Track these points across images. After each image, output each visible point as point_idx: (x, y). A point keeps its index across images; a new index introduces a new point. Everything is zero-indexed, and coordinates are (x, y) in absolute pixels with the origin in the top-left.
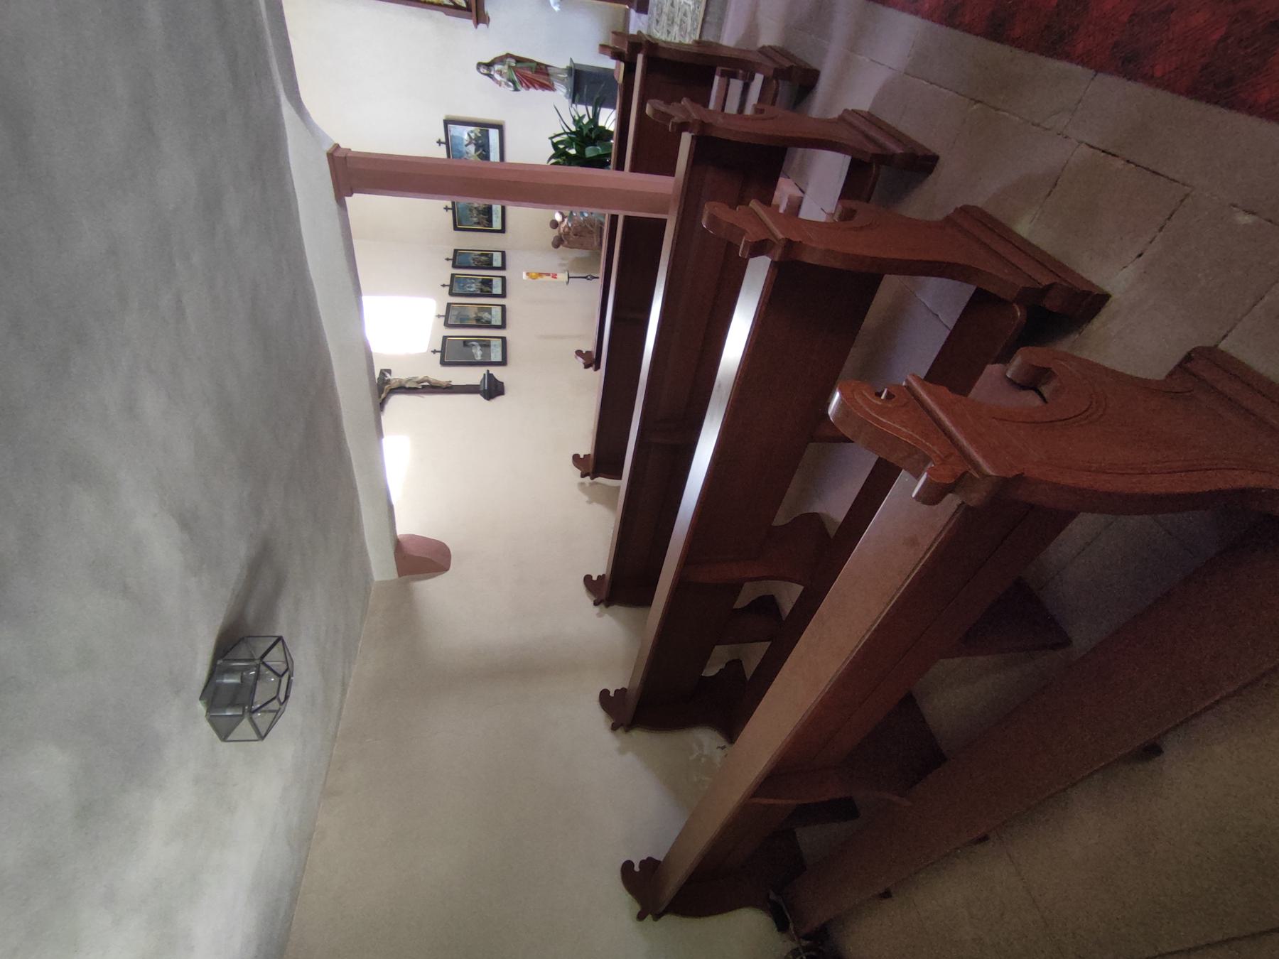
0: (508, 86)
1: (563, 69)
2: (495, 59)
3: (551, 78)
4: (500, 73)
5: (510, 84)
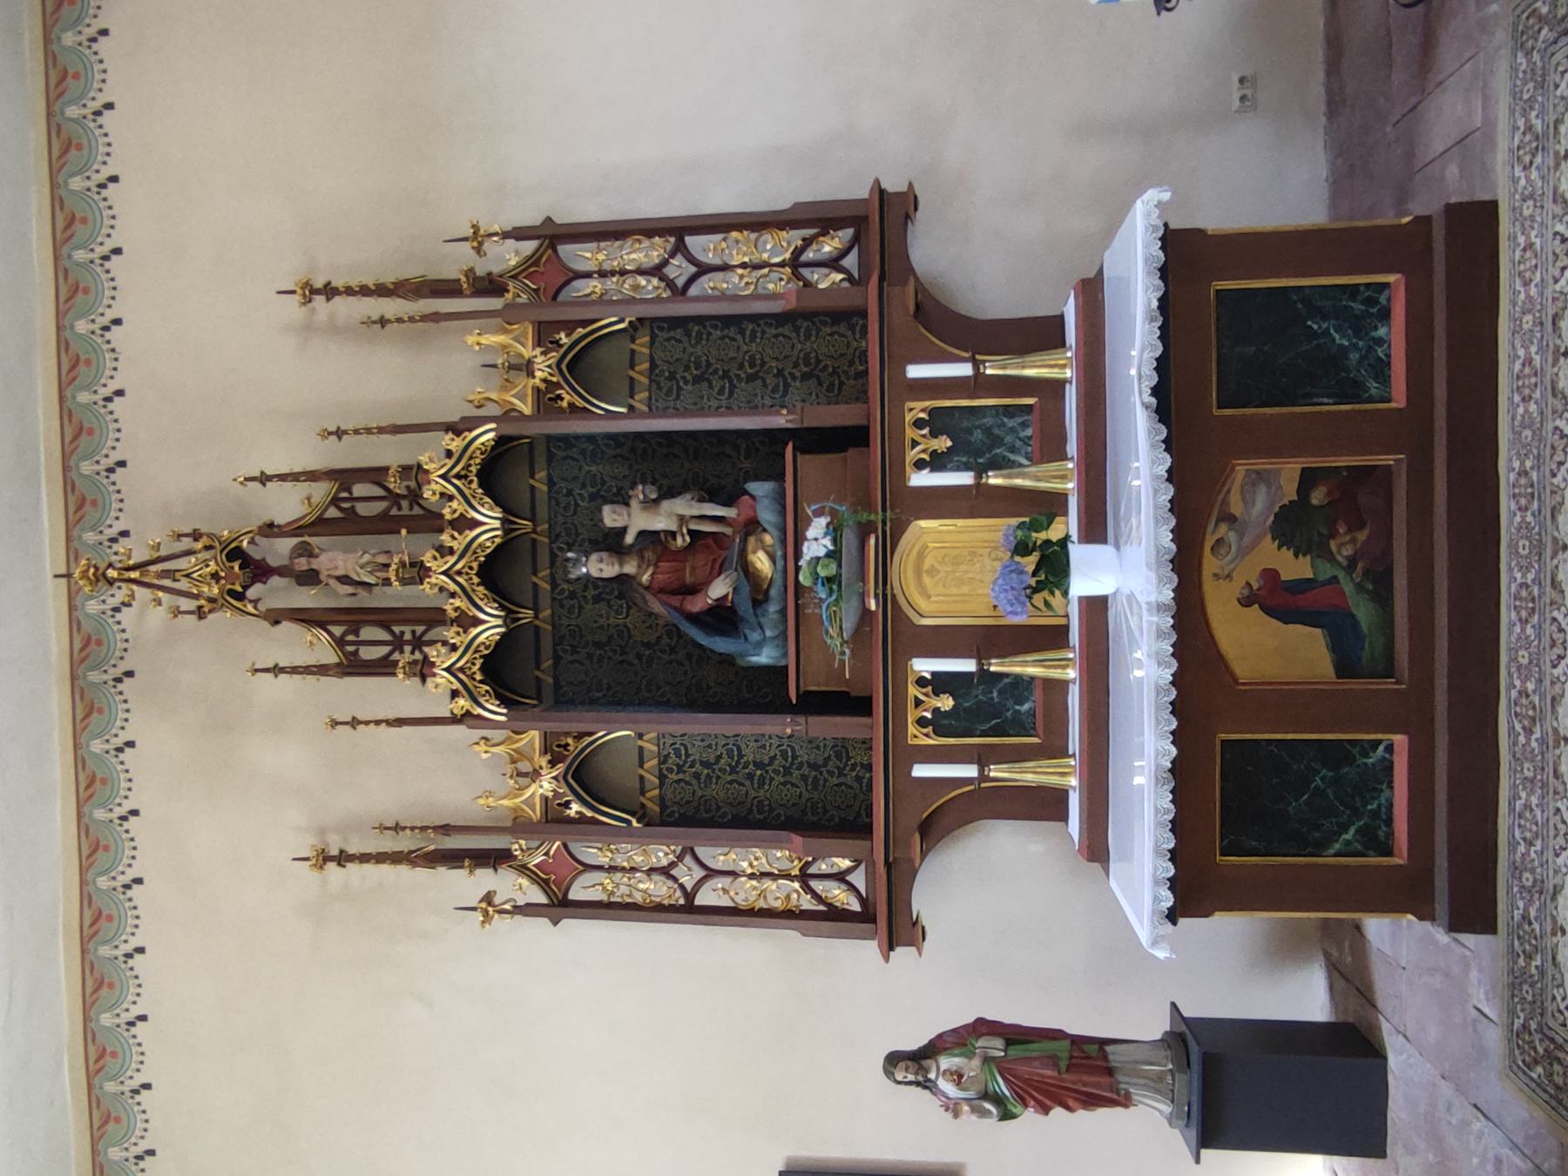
0: (984, 1113)
4: (957, 1077)
5: (988, 1106)
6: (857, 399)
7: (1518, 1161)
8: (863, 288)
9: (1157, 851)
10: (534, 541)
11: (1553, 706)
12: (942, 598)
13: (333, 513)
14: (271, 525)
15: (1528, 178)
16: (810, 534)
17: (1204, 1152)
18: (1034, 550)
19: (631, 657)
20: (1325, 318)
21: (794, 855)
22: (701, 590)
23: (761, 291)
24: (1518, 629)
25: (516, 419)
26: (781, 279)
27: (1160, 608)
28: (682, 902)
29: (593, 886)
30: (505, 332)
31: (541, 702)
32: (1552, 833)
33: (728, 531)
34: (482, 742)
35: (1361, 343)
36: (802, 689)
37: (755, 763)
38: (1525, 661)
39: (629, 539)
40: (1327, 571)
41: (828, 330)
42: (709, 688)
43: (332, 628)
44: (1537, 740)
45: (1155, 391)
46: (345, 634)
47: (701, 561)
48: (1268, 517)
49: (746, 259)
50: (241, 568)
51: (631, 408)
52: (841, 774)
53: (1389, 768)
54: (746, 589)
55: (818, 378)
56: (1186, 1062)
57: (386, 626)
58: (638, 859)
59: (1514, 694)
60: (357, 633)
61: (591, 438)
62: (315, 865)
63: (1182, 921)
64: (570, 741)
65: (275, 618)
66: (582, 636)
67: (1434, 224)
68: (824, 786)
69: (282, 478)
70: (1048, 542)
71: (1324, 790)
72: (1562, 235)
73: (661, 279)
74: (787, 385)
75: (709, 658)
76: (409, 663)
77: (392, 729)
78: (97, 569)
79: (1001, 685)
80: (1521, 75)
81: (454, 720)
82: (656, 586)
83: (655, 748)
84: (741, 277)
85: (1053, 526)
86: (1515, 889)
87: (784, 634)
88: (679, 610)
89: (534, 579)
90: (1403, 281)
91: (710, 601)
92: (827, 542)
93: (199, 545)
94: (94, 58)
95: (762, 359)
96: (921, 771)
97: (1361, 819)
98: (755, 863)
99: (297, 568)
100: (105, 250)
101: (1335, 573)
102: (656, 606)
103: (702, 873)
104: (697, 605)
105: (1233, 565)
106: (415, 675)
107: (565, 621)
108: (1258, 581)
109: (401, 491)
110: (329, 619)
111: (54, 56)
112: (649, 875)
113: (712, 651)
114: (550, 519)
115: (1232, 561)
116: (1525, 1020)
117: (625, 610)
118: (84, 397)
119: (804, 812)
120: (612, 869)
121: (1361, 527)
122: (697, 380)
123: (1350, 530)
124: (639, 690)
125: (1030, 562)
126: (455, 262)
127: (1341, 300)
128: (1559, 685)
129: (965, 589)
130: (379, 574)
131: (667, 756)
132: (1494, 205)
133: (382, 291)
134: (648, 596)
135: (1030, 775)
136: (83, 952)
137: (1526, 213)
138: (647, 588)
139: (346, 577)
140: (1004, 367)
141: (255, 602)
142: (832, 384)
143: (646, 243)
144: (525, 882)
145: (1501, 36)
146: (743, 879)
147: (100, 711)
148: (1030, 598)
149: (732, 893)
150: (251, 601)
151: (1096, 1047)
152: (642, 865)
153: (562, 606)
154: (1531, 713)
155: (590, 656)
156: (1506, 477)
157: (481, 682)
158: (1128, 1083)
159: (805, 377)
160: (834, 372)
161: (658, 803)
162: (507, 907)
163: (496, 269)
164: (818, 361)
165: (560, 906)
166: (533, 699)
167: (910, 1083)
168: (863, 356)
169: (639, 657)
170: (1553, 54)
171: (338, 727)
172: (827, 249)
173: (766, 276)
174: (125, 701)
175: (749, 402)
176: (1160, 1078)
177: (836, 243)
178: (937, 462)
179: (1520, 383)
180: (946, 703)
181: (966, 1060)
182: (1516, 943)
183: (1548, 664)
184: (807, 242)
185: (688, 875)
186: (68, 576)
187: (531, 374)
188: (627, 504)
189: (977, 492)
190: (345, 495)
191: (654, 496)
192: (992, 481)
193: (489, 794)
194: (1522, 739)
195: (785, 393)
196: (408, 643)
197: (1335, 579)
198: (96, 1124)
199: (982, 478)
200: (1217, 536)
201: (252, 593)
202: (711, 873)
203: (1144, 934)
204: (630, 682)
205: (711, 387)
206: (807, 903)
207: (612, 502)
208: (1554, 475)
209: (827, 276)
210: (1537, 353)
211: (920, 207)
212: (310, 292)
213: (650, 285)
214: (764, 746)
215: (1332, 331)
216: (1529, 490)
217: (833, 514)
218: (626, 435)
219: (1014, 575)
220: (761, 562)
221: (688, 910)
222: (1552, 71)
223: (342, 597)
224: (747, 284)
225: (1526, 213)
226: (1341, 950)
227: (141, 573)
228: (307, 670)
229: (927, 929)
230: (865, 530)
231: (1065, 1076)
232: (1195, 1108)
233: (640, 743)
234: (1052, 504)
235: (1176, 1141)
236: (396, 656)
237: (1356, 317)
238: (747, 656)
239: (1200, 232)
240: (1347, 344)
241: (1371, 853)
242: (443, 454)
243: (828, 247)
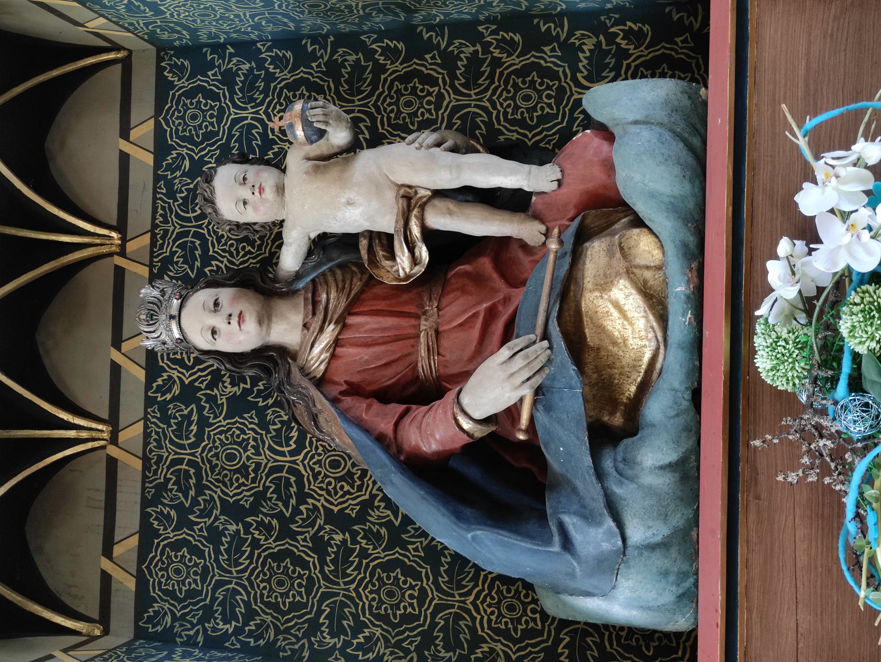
82: (341, 378)
114: (154, 226)
153: (165, 419)
188: (279, 164)
204: (296, 606)
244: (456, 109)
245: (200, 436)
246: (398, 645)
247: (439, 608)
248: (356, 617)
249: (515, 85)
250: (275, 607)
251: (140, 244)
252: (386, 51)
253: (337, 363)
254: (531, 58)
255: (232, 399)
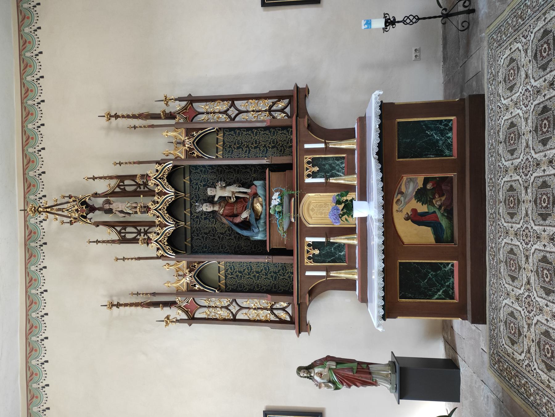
0: (329, 387)
1: (386, 365)
2: (315, 361)
3: (374, 376)
4: (320, 375)
5: (330, 384)
6: (290, 154)
7: (492, 396)
8: (291, 119)
9: (379, 297)
10: (185, 200)
11: (499, 251)
12: (316, 218)
13: (118, 190)
14: (96, 194)
15: (492, 89)
16: (273, 198)
17: (400, 400)
18: (342, 203)
19: (216, 237)
20: (432, 130)
21: (268, 302)
22: (239, 216)
23: (259, 120)
24: (490, 228)
25: (178, 160)
26: (265, 116)
27: (379, 220)
28: (232, 318)
29: (203, 313)
30: (176, 131)
31: (186, 252)
32: (499, 290)
33: (248, 196)
34: (167, 265)
35: (443, 138)
36: (271, 248)
37: (256, 272)
38: (492, 238)
39: (216, 199)
40: (432, 209)
41: (281, 132)
42: (242, 247)
43: (116, 228)
44: (495, 262)
45: (377, 154)
46: (121, 230)
47: (239, 206)
48: (413, 192)
49: (254, 109)
50: (86, 208)
51: (217, 157)
52: (284, 275)
53: (452, 272)
54: (253, 216)
55: (277, 148)
56: (395, 371)
57: (135, 227)
58: (218, 303)
59: (490, 248)
60: (125, 230)
61: (204, 166)
62: (109, 307)
63: (387, 320)
64: (196, 264)
65: (97, 224)
66: (200, 231)
67: (466, 101)
68: (278, 279)
69: (101, 178)
70: (347, 200)
71: (432, 278)
72: (499, 106)
73: (226, 115)
74: (267, 150)
75: (242, 238)
76: (143, 239)
77: (137, 261)
78: (35, 208)
79: (335, 246)
80: (490, 56)
81: (158, 258)
83: (224, 267)
84: (253, 115)
85: (348, 195)
86: (491, 309)
87: (265, 230)
88: (232, 222)
89: (185, 212)
90: (456, 119)
91: (242, 219)
92: (278, 200)
93: (71, 200)
94: (35, 37)
95: (259, 141)
96: (308, 273)
97: (444, 288)
98: (256, 305)
99: (105, 208)
100: (39, 101)
101: (435, 210)
102: (224, 220)
103: (239, 308)
104: (238, 220)
105: (402, 208)
106: (145, 243)
107: (195, 226)
108: (410, 212)
109: (142, 183)
110: (116, 225)
111: (22, 36)
112: (221, 309)
113: (243, 236)
115: (403, 206)
116: (493, 351)
117: (214, 222)
118: (31, 150)
119: (272, 288)
120: (209, 307)
121: (443, 195)
122: (238, 148)
123: (439, 197)
124: (219, 248)
125: (341, 207)
126: (160, 107)
127: (437, 125)
128: (500, 245)
129: (323, 216)
130: (133, 210)
131: (228, 270)
132: (484, 94)
133: (134, 117)
134: (222, 217)
135: (343, 275)
136: (26, 339)
137: (491, 99)
138: (222, 215)
139: (122, 211)
140: (335, 145)
141: (90, 219)
142: (281, 150)
143: (222, 103)
144: (180, 312)
145: (485, 44)
146: (252, 310)
147: (35, 256)
148: (341, 218)
149: (248, 315)
150: (89, 219)
151: (366, 365)
152: (219, 305)
153: (194, 221)
154: (494, 254)
155: (203, 237)
156: (487, 180)
157: (167, 245)
158: (376, 377)
159: (273, 147)
160: (282, 146)
161: (224, 285)
162: (174, 320)
163: (173, 111)
164: (277, 142)
165: (192, 319)
166: (184, 251)
167: (305, 377)
168: (291, 141)
169: (219, 237)
170: (497, 51)
171: (118, 260)
172: (280, 106)
173: (261, 114)
174: (43, 253)
175: (255, 155)
176: (387, 376)
177: (283, 104)
178: (314, 175)
179: (490, 151)
180: (317, 252)
181: (323, 369)
182: (491, 326)
183: (498, 238)
184: (274, 104)
185: (234, 308)
186: (25, 210)
187: (184, 145)
188: (215, 188)
189: (326, 185)
190: (122, 184)
191: (224, 185)
192: (331, 181)
193: (168, 282)
194: (492, 262)
195: (266, 152)
196: (142, 233)
197: (434, 212)
198: (29, 399)
199: (328, 180)
200: (398, 198)
201: (89, 216)
202: (242, 308)
203: (375, 323)
204: (216, 246)
205: (243, 150)
206: (273, 318)
207: (211, 187)
208: (498, 180)
209: (280, 115)
210: (494, 142)
211: (310, 93)
212: (110, 116)
213: (223, 117)
214: (259, 266)
215: (434, 134)
216: (492, 184)
217: (281, 191)
218: (215, 166)
219: (335, 211)
220: (258, 207)
221: (234, 320)
222: (497, 56)
223: (120, 218)
224: (254, 117)
225: (491, 99)
226: (447, 336)
227: (49, 209)
228: (108, 242)
229: (312, 327)
230: (291, 196)
231: (355, 375)
232: (397, 386)
233: (219, 265)
234: (349, 188)
235: (393, 397)
236: (138, 237)
237: (442, 130)
238: (254, 237)
239: (392, 104)
240: (438, 138)
241: (448, 299)
242: (155, 171)
243: (281, 105)
244: (236, 177)
245: (200, 223)
246: (231, 249)
247: (236, 244)
248: (225, 246)
249: (244, 174)
250: (213, 246)
251: (188, 195)
252: (225, 168)
253: (224, 213)
254: (246, 170)
255: (204, 218)
